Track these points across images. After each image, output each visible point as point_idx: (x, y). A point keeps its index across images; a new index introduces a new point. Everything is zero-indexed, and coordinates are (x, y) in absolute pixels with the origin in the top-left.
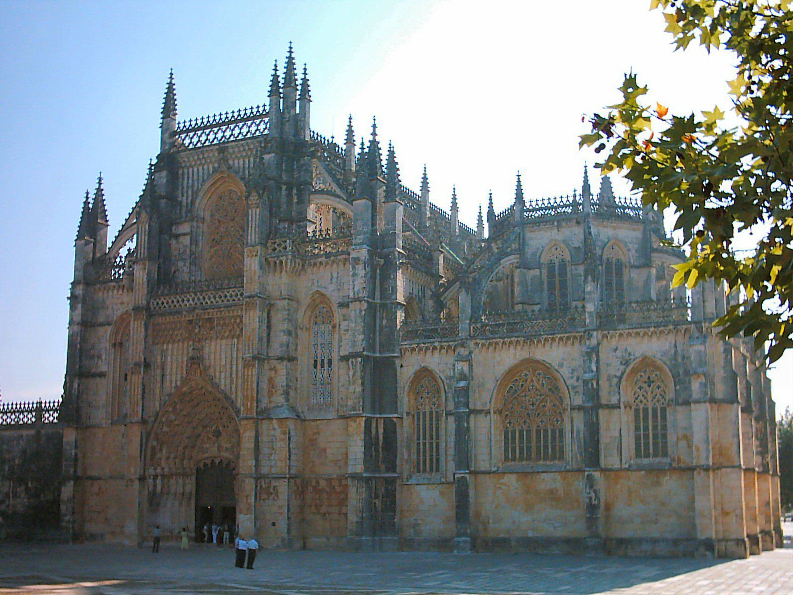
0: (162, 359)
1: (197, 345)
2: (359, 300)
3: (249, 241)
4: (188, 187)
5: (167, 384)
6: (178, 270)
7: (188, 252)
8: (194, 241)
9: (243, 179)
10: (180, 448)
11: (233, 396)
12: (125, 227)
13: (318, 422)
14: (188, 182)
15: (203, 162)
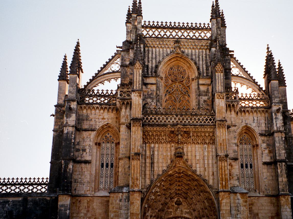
0: (150, 153)
1: (180, 146)
2: (281, 132)
3: (217, 90)
4: (152, 58)
5: (156, 168)
6: (147, 103)
7: (155, 94)
8: (158, 88)
9: (192, 59)
10: (157, 211)
11: (207, 178)
12: (98, 75)
13: (252, 198)
14: (152, 55)
15: (163, 46)
